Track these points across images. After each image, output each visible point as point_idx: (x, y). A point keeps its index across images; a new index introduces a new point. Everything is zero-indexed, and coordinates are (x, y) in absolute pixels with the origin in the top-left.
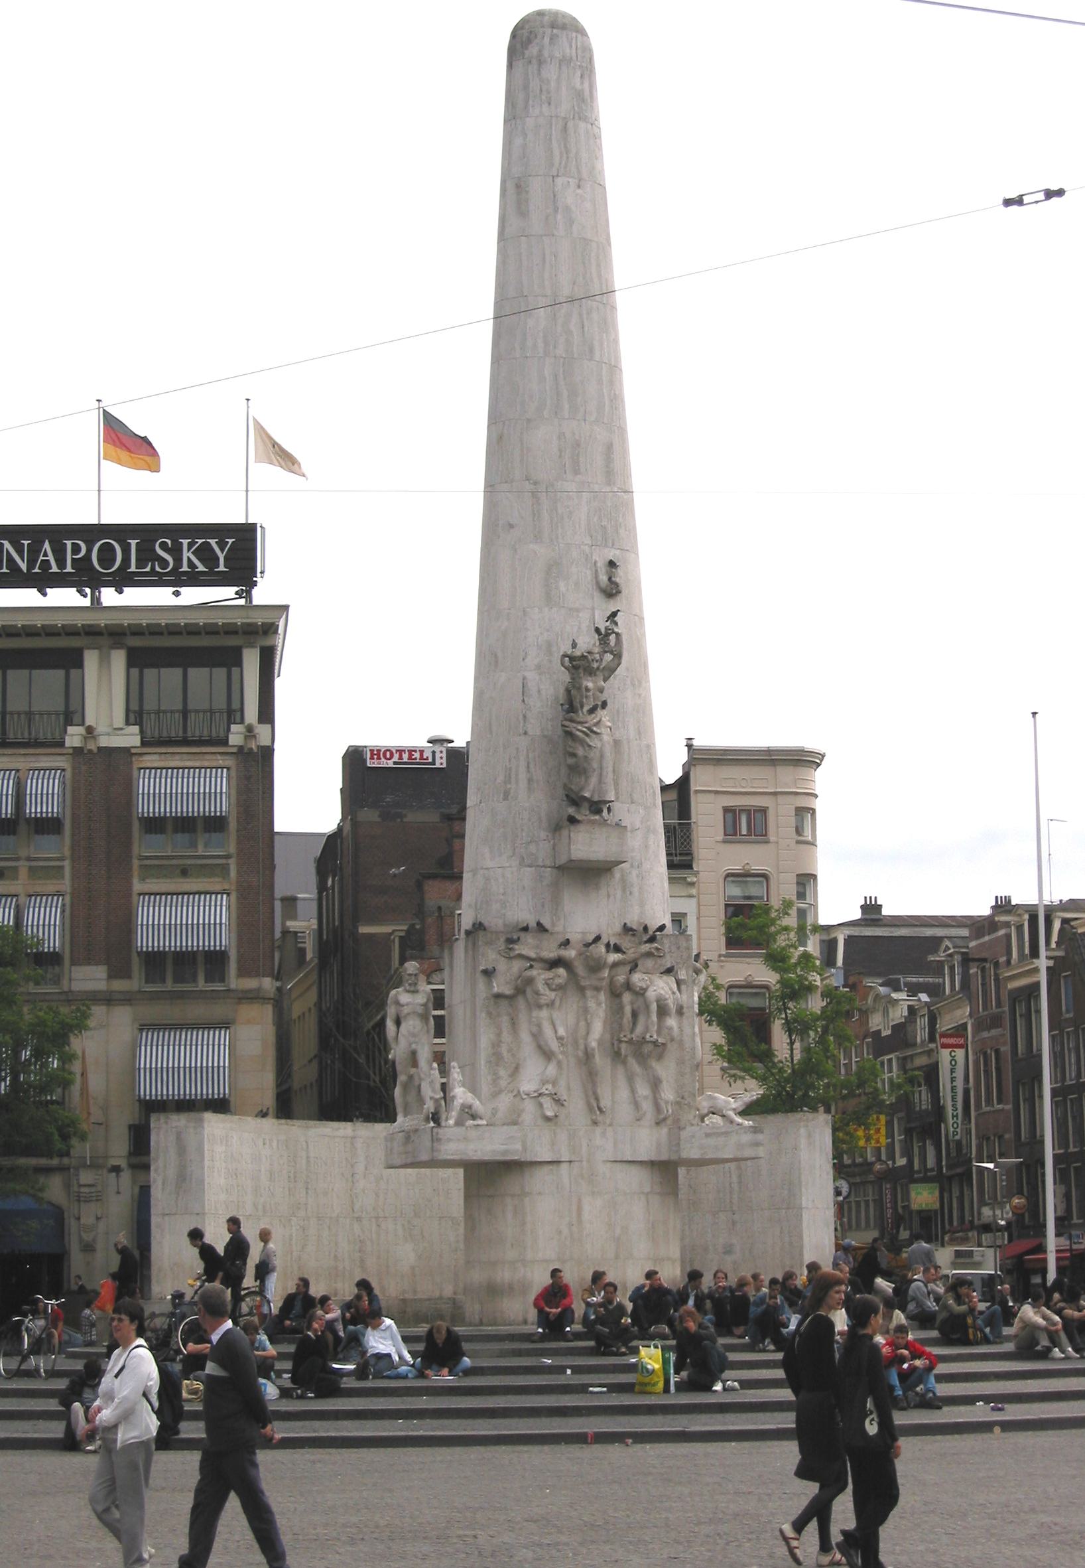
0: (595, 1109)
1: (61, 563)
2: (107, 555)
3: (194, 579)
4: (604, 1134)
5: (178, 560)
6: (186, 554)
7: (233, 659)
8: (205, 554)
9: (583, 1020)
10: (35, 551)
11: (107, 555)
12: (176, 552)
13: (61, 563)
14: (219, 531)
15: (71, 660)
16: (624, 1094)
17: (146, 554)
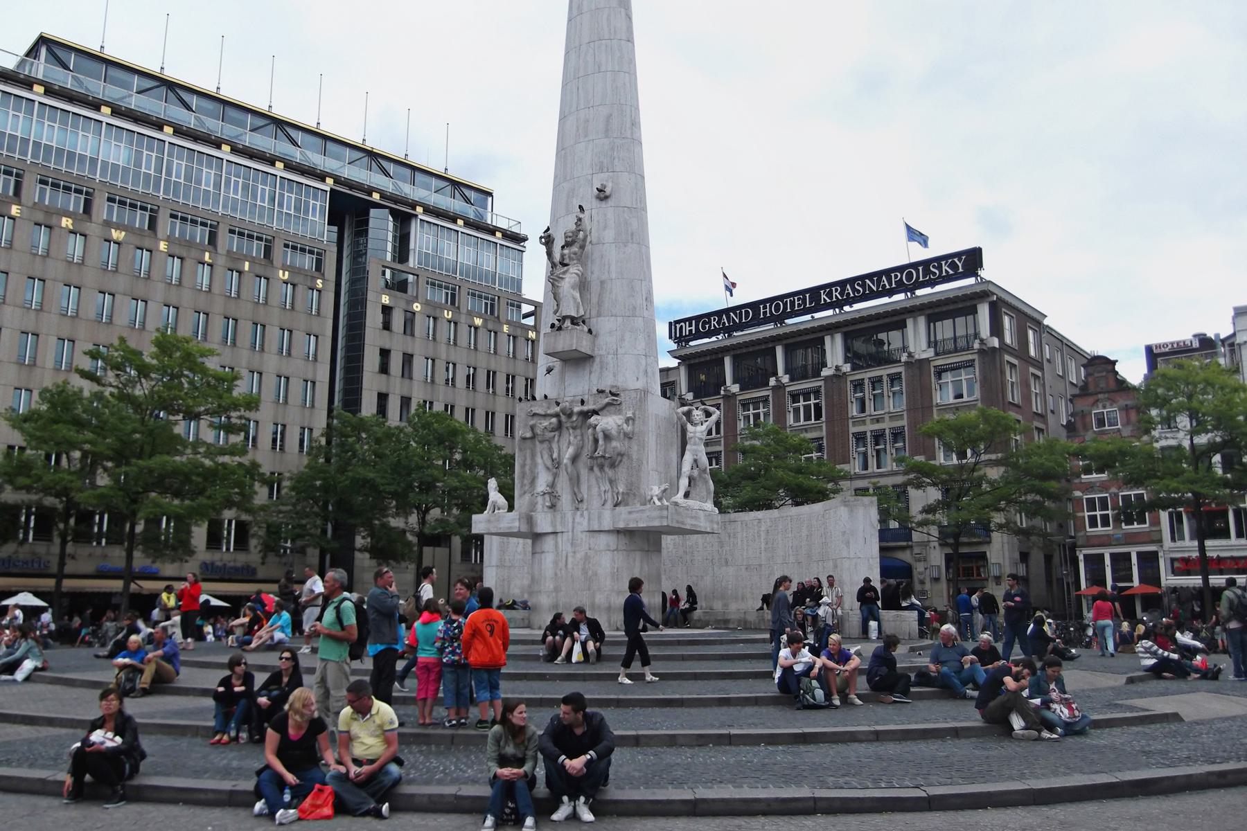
0: (578, 501)
1: (890, 284)
2: (910, 276)
3: (948, 279)
4: (582, 515)
5: (941, 272)
6: (945, 268)
7: (973, 311)
8: (953, 266)
10: (879, 280)
11: (910, 276)
12: (940, 268)
13: (890, 284)
14: (958, 255)
15: (902, 326)
16: (595, 490)
17: (927, 272)
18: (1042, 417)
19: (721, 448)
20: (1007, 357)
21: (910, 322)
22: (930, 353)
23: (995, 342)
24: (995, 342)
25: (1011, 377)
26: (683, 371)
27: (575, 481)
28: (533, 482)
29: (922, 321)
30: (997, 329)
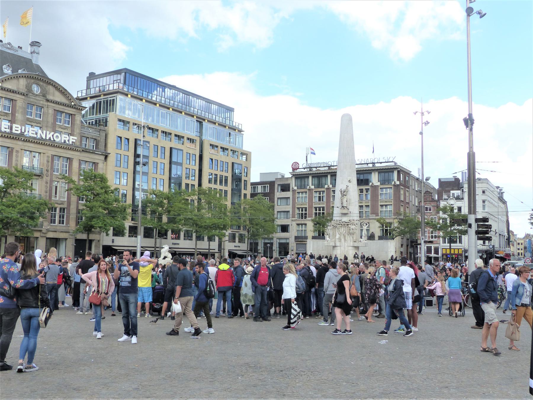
0: (345, 240)
9: (343, 230)
18: (408, 203)
19: (307, 206)
20: (401, 187)
21: (373, 174)
22: (379, 184)
23: (398, 183)
24: (398, 183)
25: (402, 192)
26: (293, 179)
27: (345, 237)
28: (335, 236)
29: (377, 174)
30: (399, 179)
